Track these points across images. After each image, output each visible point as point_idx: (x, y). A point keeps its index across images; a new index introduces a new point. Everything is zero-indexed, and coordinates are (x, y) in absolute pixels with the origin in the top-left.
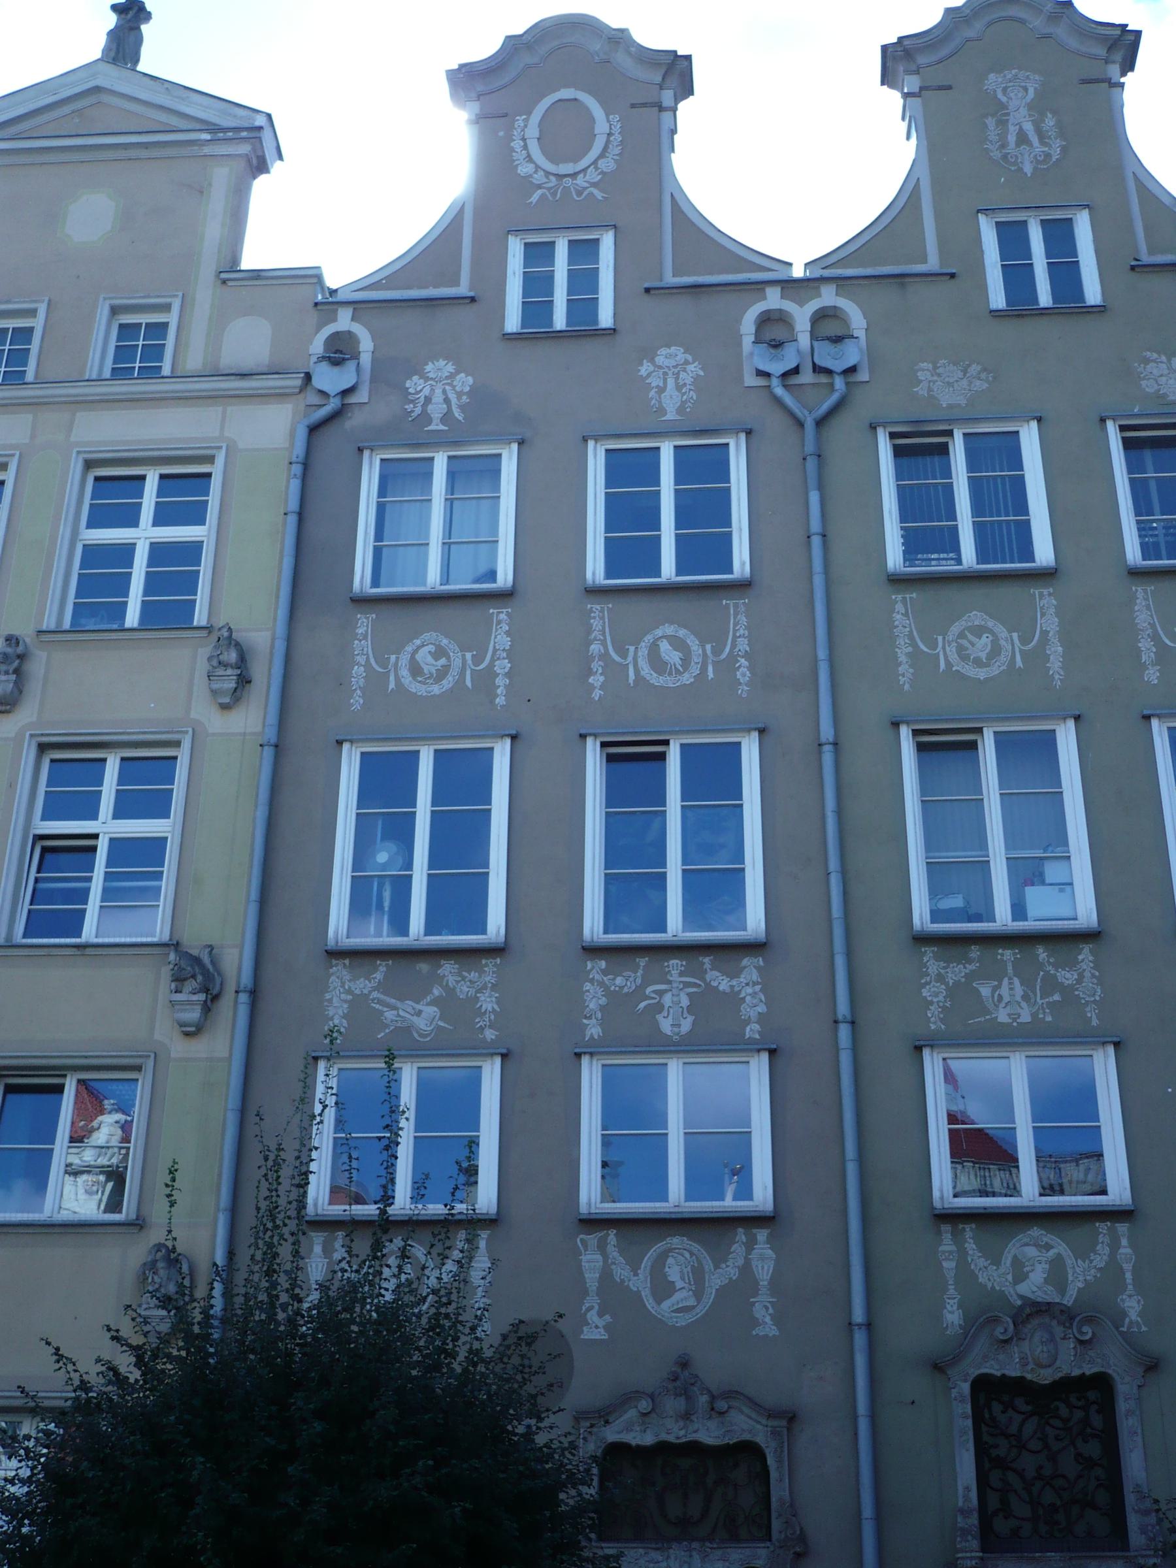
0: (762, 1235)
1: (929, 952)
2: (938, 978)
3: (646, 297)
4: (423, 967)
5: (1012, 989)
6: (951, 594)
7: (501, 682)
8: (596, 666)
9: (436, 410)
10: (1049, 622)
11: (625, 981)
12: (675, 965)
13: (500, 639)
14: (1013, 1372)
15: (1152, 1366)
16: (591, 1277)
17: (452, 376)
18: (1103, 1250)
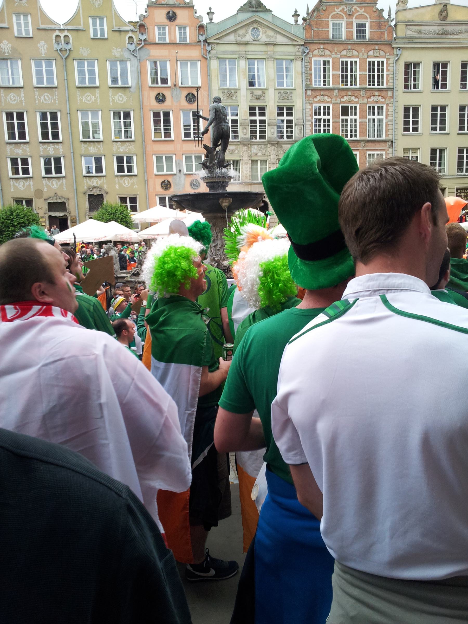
0: (64, 178)
1: (82, 143)
2: (84, 146)
3: (37, 30)
4: (19, 145)
5: (92, 148)
6: (85, 90)
7: (23, 102)
8: (37, 100)
9: (6, 51)
10: (98, 95)
11: (45, 146)
12: (51, 144)
13: (22, 95)
14: (92, 194)
15: (107, 193)
16: (44, 184)
17: (8, 44)
18: (102, 180)
